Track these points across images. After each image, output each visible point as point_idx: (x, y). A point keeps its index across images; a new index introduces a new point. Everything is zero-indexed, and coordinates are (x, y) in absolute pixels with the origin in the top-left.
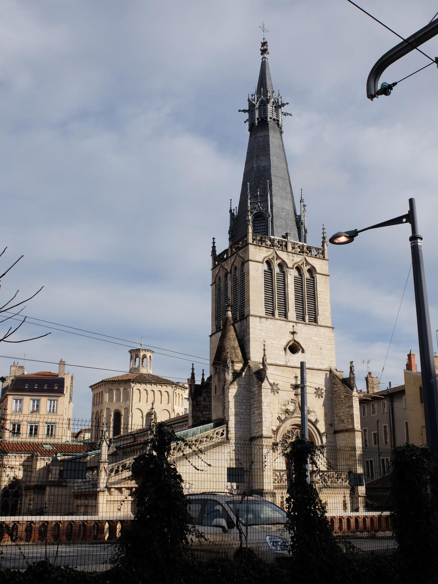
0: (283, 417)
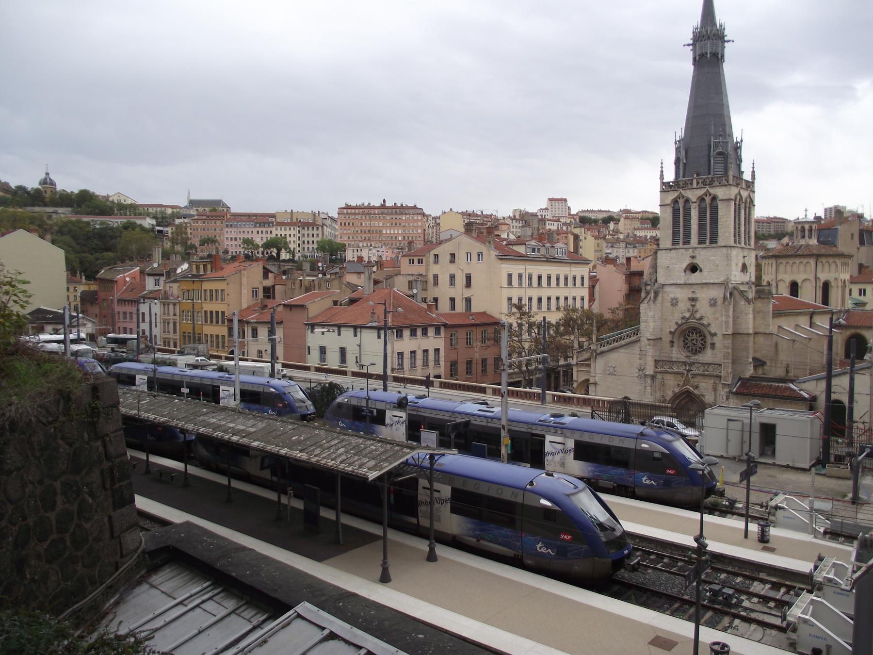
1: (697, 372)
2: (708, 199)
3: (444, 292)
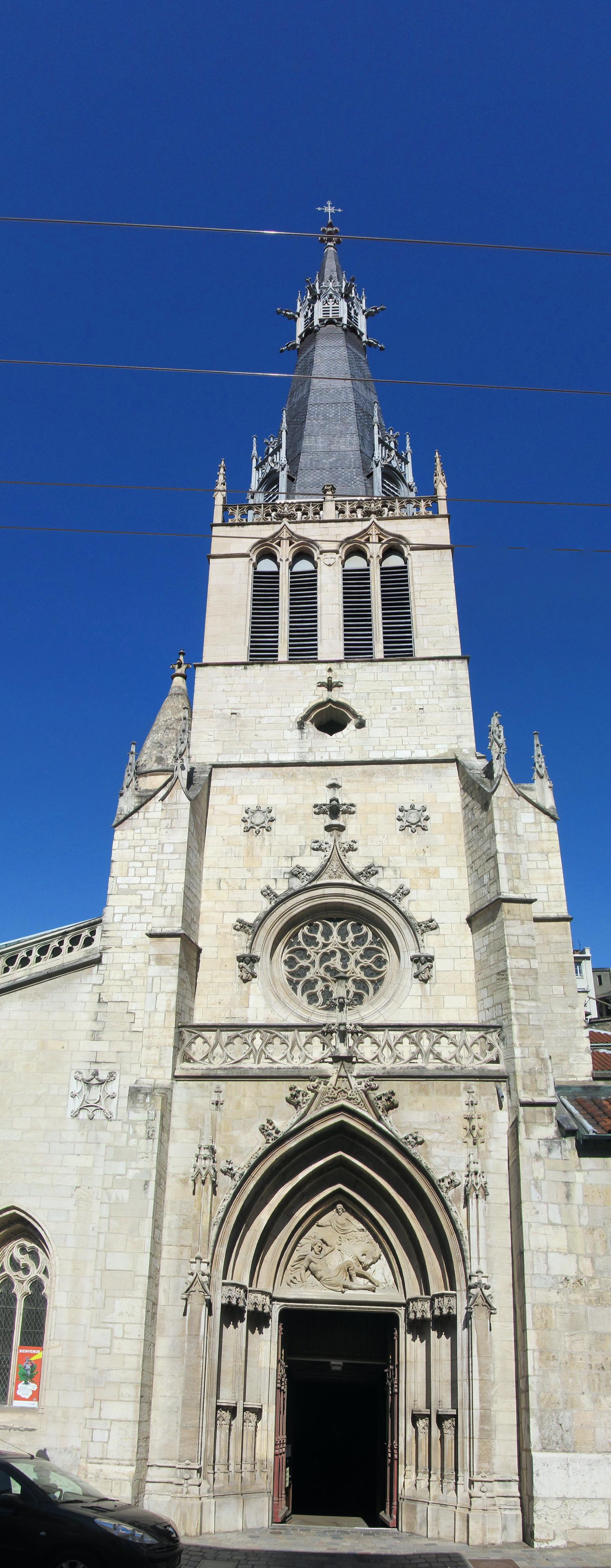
1: (388, 1064)
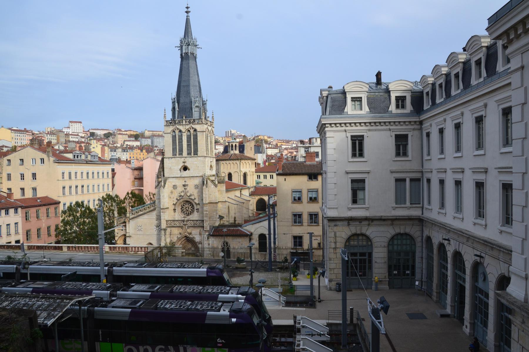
0: (179, 198)
2: (192, 131)
3: (15, 185)
